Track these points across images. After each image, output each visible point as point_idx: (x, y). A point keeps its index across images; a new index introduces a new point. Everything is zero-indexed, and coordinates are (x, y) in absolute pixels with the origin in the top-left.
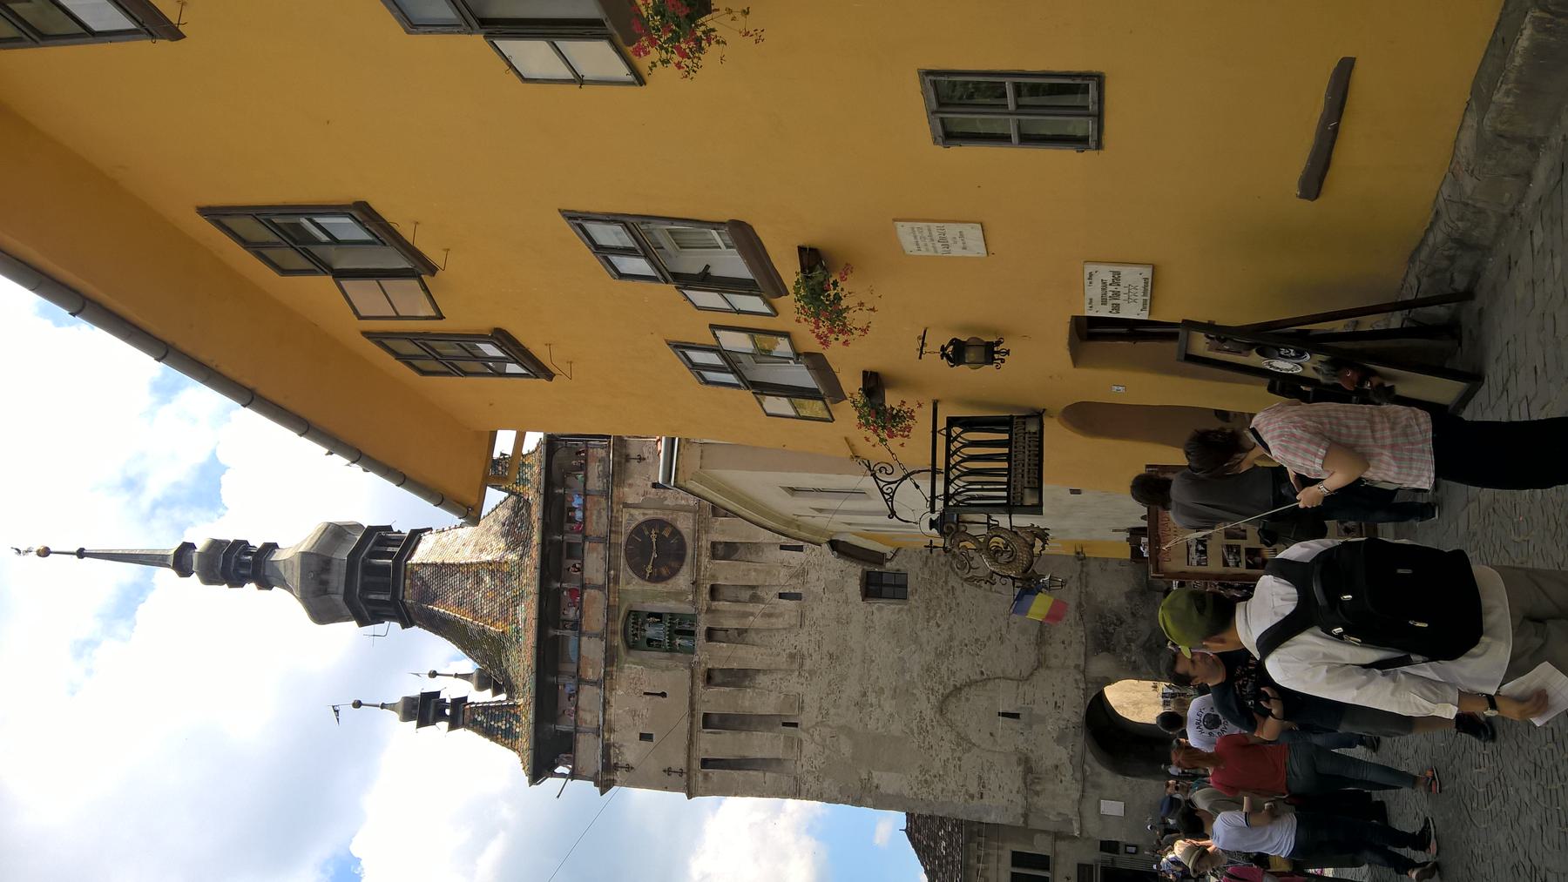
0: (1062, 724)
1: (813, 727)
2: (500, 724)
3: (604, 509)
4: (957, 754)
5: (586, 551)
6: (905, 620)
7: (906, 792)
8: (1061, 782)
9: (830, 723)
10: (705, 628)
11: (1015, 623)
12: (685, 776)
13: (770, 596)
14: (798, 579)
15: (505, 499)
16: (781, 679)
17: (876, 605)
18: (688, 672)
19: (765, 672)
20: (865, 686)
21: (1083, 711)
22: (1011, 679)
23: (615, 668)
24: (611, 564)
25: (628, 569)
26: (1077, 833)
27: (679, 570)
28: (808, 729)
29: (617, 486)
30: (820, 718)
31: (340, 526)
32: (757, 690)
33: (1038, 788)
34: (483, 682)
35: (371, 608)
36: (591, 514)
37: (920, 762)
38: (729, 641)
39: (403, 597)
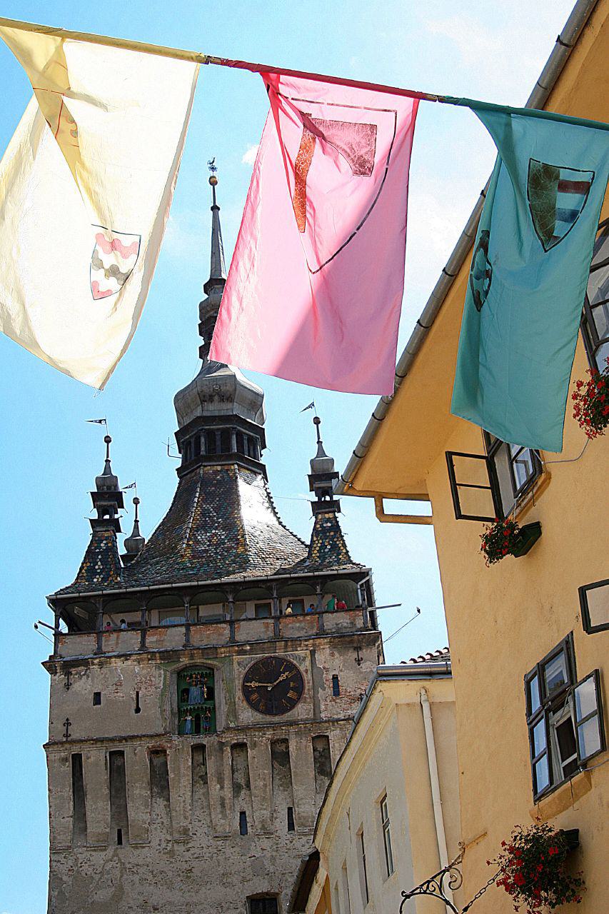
1: (120, 860)
2: (99, 563)
5: (265, 621)
9: (125, 876)
10: (204, 743)
12: (64, 740)
13: (242, 803)
15: (303, 543)
16: (163, 823)
18: (161, 731)
23: (158, 662)
24: (256, 645)
27: (257, 710)
28: (117, 856)
30: (128, 866)
31: (261, 405)
34: (133, 542)
35: (193, 440)
36: (300, 622)
39: (205, 466)
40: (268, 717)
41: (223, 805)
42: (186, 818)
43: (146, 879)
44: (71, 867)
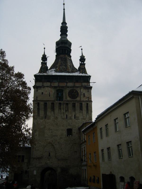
4: (42, 146)
9: (46, 124)
10: (61, 102)
12: (36, 100)
13: (67, 113)
18: (53, 100)
19: (54, 113)
24: (71, 87)
25: (70, 90)
41: (63, 113)
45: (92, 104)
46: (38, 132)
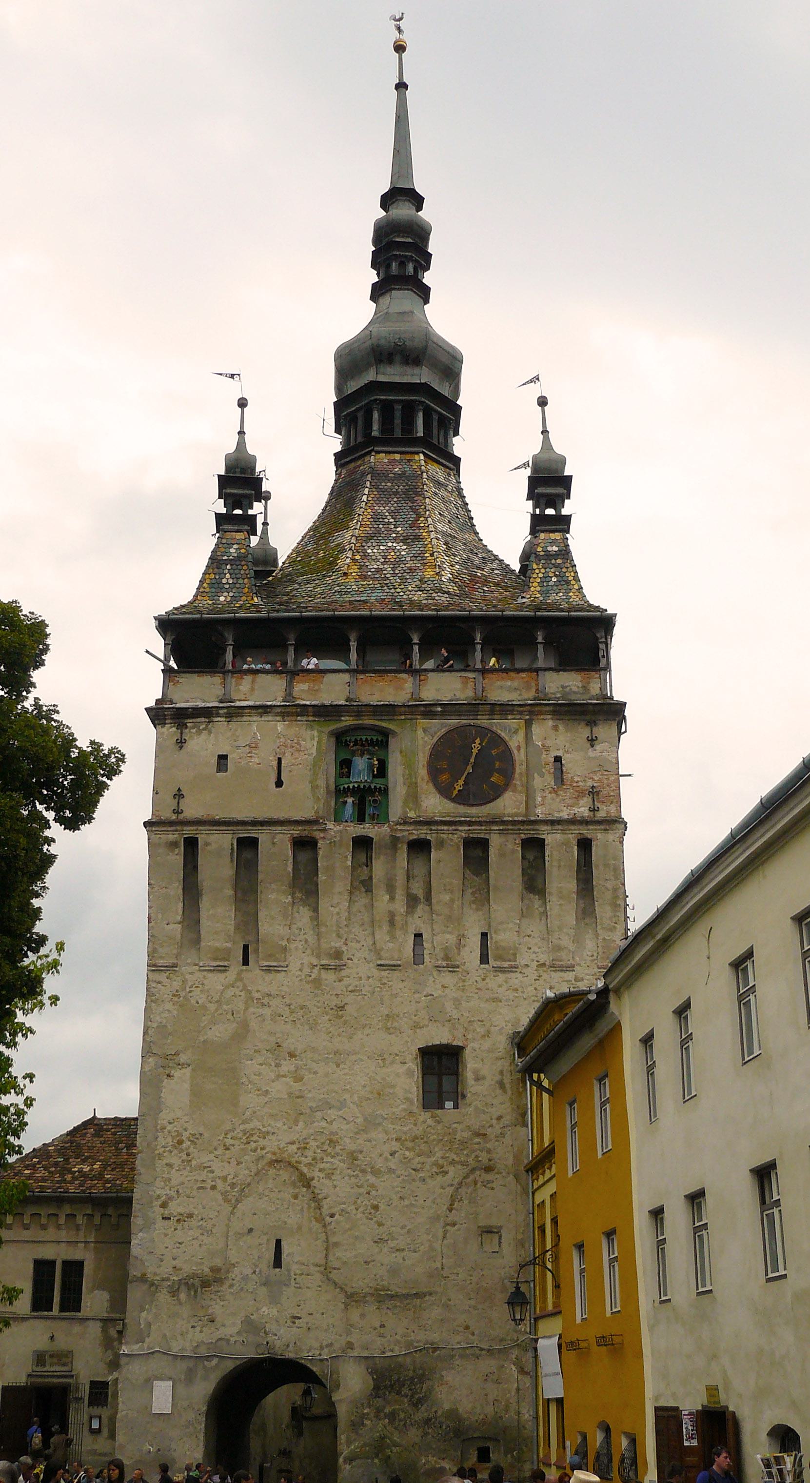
0: (271, 1327)
1: (245, 986)
3: (520, 695)
4: (220, 1184)
6: (397, 1107)
7: (164, 1117)
8: (193, 1327)
9: (251, 1010)
10: (370, 835)
11: (404, 1260)
12: (174, 817)
13: (418, 921)
14: (443, 960)
16: (306, 941)
17: (414, 1066)
18: (309, 815)
20: (303, 1055)
21: (291, 1355)
22: (326, 1256)
23: (311, 718)
24: (449, 709)
25: (444, 731)
26: (125, 1349)
27: (446, 797)
28: (241, 980)
29: (554, 711)
30: (256, 995)
32: (290, 908)
33: (183, 1296)
35: (360, 415)
36: (512, 679)
37: (206, 1135)
38: (353, 868)
39: (378, 452)
40: (462, 807)
42: (339, 936)
43: (280, 1016)
44: (177, 991)
45: (622, 842)
46: (187, 1071)
